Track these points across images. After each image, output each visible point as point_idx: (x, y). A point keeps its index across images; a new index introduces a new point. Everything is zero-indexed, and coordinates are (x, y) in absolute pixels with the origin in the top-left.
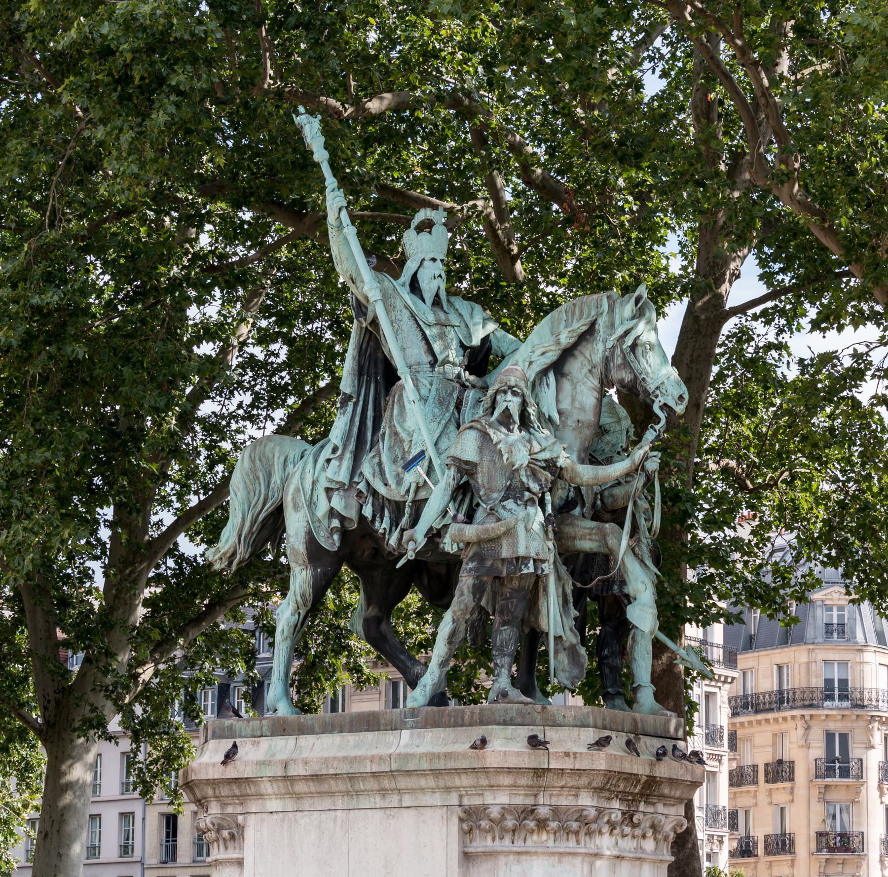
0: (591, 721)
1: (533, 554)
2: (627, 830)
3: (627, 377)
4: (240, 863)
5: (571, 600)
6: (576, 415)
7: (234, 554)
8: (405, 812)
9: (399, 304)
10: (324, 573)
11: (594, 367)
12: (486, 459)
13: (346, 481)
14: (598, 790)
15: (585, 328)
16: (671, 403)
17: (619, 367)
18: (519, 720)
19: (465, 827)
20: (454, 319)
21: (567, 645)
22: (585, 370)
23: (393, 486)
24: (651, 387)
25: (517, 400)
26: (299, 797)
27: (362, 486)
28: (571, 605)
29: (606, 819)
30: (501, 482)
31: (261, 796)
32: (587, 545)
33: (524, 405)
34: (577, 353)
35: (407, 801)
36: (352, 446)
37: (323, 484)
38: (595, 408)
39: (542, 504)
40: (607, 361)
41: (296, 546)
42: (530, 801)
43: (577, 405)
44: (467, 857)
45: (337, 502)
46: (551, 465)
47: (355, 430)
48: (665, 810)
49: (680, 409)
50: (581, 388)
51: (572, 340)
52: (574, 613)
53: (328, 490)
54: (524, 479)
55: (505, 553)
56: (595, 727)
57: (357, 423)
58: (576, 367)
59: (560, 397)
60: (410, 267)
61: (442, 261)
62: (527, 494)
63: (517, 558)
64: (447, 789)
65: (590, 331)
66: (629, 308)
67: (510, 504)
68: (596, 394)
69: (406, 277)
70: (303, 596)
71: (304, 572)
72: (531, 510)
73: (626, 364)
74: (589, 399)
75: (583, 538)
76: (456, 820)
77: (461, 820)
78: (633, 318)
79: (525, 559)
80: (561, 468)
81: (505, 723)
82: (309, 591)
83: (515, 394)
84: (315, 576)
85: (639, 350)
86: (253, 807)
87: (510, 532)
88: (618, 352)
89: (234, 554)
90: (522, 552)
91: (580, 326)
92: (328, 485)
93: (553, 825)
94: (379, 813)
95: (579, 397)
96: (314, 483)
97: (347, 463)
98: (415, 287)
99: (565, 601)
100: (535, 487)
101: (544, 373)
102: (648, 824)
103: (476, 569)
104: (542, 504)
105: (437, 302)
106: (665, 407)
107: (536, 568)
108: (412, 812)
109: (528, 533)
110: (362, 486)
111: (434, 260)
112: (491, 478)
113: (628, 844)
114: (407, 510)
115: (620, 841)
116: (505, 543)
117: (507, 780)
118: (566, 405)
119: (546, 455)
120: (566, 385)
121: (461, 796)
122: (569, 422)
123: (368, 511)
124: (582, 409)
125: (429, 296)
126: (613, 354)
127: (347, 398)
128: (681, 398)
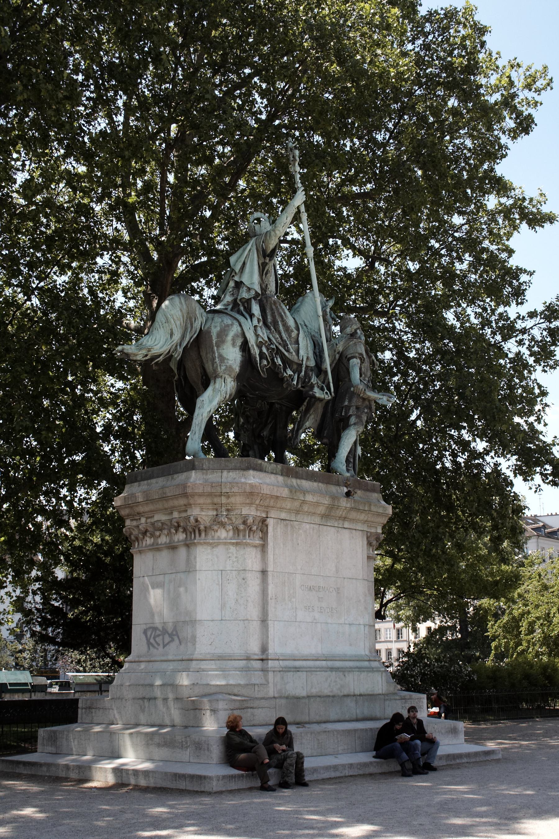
4: (263, 548)
7: (160, 355)
8: (344, 530)
23: (294, 353)
27: (275, 347)
35: (346, 525)
41: (234, 367)
45: (264, 350)
70: (230, 395)
71: (233, 383)
89: (160, 355)
92: (260, 340)
94: (333, 529)
108: (347, 531)
110: (275, 347)
114: (304, 369)
123: (279, 362)
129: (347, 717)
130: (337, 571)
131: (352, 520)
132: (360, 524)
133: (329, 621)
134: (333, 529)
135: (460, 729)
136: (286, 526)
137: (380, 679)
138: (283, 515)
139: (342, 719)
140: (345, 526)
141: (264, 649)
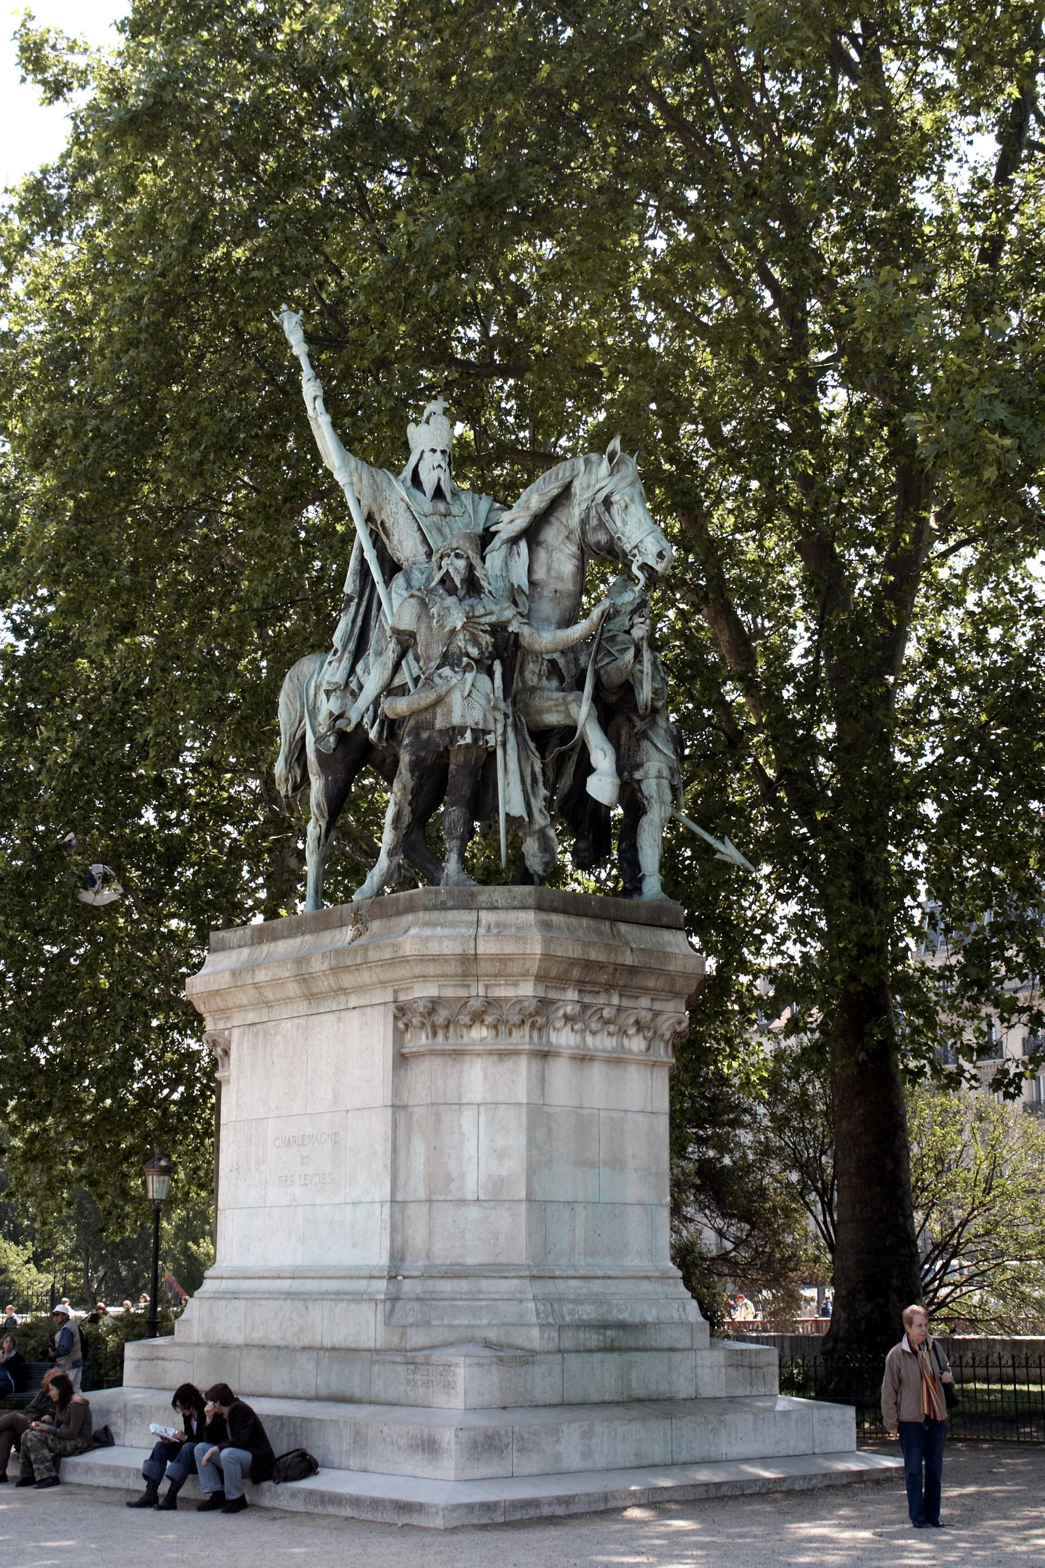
0: (531, 901)
1: (470, 722)
2: (594, 1026)
3: (602, 538)
5: (540, 779)
6: (553, 585)
9: (394, 498)
10: (335, 781)
11: (571, 532)
12: (423, 626)
13: (342, 682)
14: (540, 978)
15: (556, 492)
16: (651, 562)
17: (595, 529)
18: (450, 904)
19: (401, 1025)
20: (455, 510)
21: (536, 827)
22: (562, 537)
24: (628, 547)
25: (461, 564)
26: (268, 1005)
28: (541, 784)
29: (561, 1013)
30: (438, 650)
31: (241, 1007)
32: (552, 718)
33: (471, 567)
34: (553, 519)
35: (353, 1001)
36: (352, 646)
37: (325, 687)
38: (575, 575)
39: (491, 674)
40: (583, 523)
42: (461, 993)
43: (553, 574)
44: (402, 1059)
46: (498, 629)
47: (357, 630)
48: (658, 1006)
49: (660, 567)
50: (557, 555)
51: (543, 505)
52: (543, 792)
53: (328, 693)
54: (461, 644)
55: (439, 724)
56: (539, 908)
57: (359, 623)
58: (551, 534)
59: (536, 567)
60: (413, 459)
61: (443, 452)
62: (465, 659)
63: (454, 728)
64: (383, 984)
65: (565, 493)
66: (605, 467)
67: (446, 671)
68: (575, 561)
69: (407, 473)
70: (318, 806)
72: (469, 676)
73: (601, 525)
74: (566, 566)
75: (549, 710)
76: (391, 1018)
77: (396, 1018)
78: (611, 474)
79: (461, 730)
80: (517, 635)
81: (435, 908)
82: (323, 800)
83: (457, 556)
84: (326, 785)
85: (615, 509)
86: (237, 1019)
87: (439, 701)
88: (593, 513)
90: (456, 720)
91: (553, 489)
93: (489, 1019)
94: (331, 1017)
95: (555, 566)
96: (317, 688)
97: (346, 663)
98: (416, 480)
99: (534, 780)
100: (474, 652)
101: (514, 541)
102: (632, 1020)
103: (411, 744)
104: (491, 674)
105: (438, 494)
106: (644, 567)
107: (475, 740)
108: (356, 1012)
109: (469, 702)
111: (434, 451)
112: (428, 646)
113: (602, 1042)
115: (589, 1039)
116: (439, 712)
117: (432, 969)
118: (540, 575)
119: (493, 619)
120: (542, 554)
121: (396, 992)
122: (545, 593)
124: (560, 578)
125: (429, 486)
126: (588, 516)
127: (350, 599)
128: (660, 555)
129: (299, 1392)
130: (335, 1098)
131: (359, 989)
132: (378, 992)
133: (318, 1201)
134: (331, 1016)
135: (445, 1445)
136: (256, 1034)
137: (371, 1317)
138: (251, 1017)
139: (291, 1393)
140: (351, 1005)
141: (397, 1256)
